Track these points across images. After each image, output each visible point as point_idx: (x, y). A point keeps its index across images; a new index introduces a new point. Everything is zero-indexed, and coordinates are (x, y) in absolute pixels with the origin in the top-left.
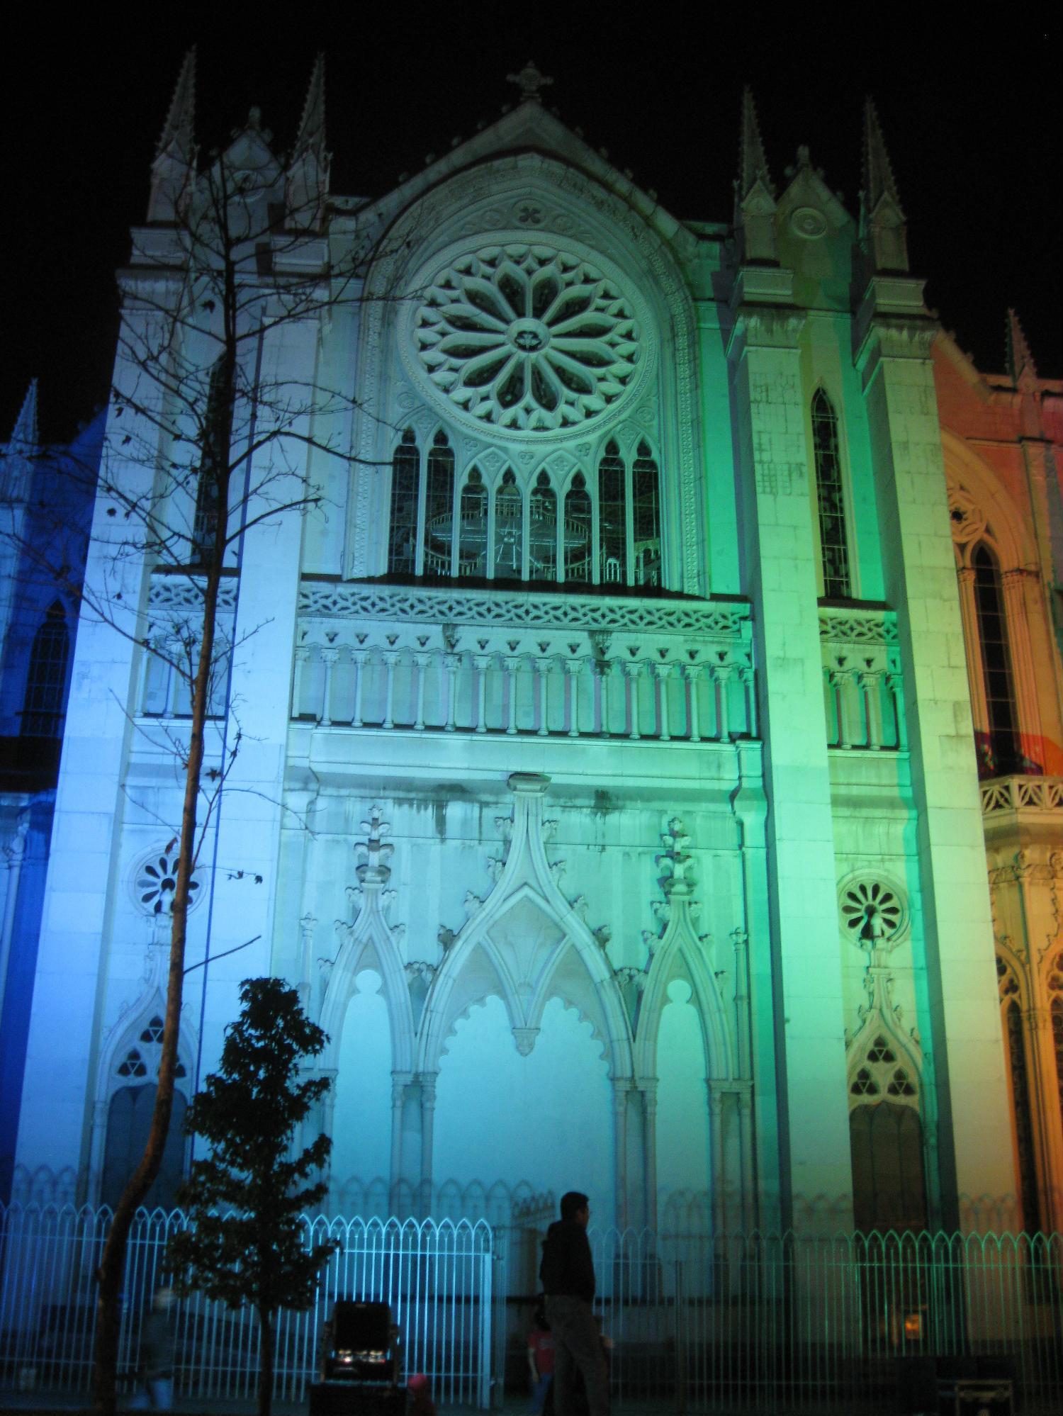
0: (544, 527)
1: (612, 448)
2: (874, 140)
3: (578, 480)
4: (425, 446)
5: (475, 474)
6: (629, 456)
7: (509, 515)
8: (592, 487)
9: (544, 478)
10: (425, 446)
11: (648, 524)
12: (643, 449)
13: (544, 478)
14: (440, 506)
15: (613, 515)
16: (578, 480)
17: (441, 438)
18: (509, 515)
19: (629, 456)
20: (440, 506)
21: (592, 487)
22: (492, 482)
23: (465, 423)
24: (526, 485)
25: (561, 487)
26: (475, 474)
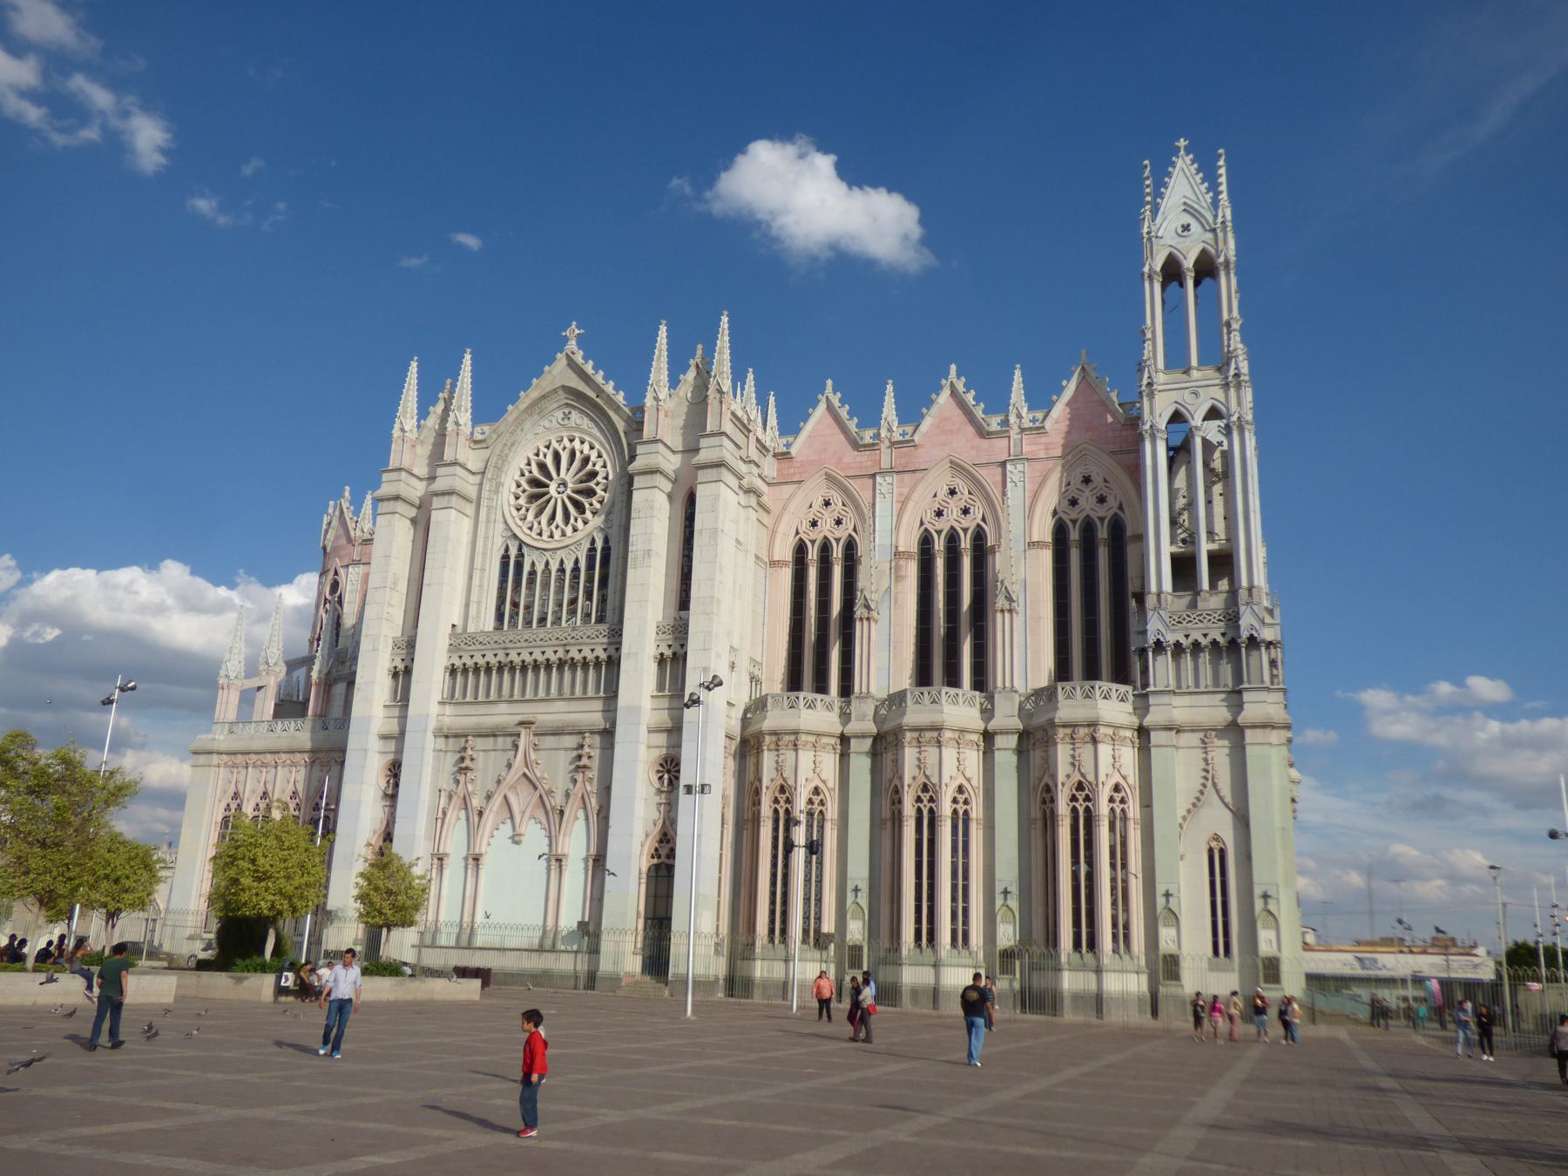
1: (593, 541)
2: (723, 342)
3: (577, 561)
4: (513, 553)
5: (533, 564)
7: (546, 585)
8: (583, 565)
9: (562, 562)
10: (513, 553)
12: (606, 540)
13: (562, 562)
16: (577, 561)
17: (520, 549)
18: (546, 585)
19: (599, 545)
22: (540, 568)
24: (554, 567)
25: (569, 566)
26: (533, 564)
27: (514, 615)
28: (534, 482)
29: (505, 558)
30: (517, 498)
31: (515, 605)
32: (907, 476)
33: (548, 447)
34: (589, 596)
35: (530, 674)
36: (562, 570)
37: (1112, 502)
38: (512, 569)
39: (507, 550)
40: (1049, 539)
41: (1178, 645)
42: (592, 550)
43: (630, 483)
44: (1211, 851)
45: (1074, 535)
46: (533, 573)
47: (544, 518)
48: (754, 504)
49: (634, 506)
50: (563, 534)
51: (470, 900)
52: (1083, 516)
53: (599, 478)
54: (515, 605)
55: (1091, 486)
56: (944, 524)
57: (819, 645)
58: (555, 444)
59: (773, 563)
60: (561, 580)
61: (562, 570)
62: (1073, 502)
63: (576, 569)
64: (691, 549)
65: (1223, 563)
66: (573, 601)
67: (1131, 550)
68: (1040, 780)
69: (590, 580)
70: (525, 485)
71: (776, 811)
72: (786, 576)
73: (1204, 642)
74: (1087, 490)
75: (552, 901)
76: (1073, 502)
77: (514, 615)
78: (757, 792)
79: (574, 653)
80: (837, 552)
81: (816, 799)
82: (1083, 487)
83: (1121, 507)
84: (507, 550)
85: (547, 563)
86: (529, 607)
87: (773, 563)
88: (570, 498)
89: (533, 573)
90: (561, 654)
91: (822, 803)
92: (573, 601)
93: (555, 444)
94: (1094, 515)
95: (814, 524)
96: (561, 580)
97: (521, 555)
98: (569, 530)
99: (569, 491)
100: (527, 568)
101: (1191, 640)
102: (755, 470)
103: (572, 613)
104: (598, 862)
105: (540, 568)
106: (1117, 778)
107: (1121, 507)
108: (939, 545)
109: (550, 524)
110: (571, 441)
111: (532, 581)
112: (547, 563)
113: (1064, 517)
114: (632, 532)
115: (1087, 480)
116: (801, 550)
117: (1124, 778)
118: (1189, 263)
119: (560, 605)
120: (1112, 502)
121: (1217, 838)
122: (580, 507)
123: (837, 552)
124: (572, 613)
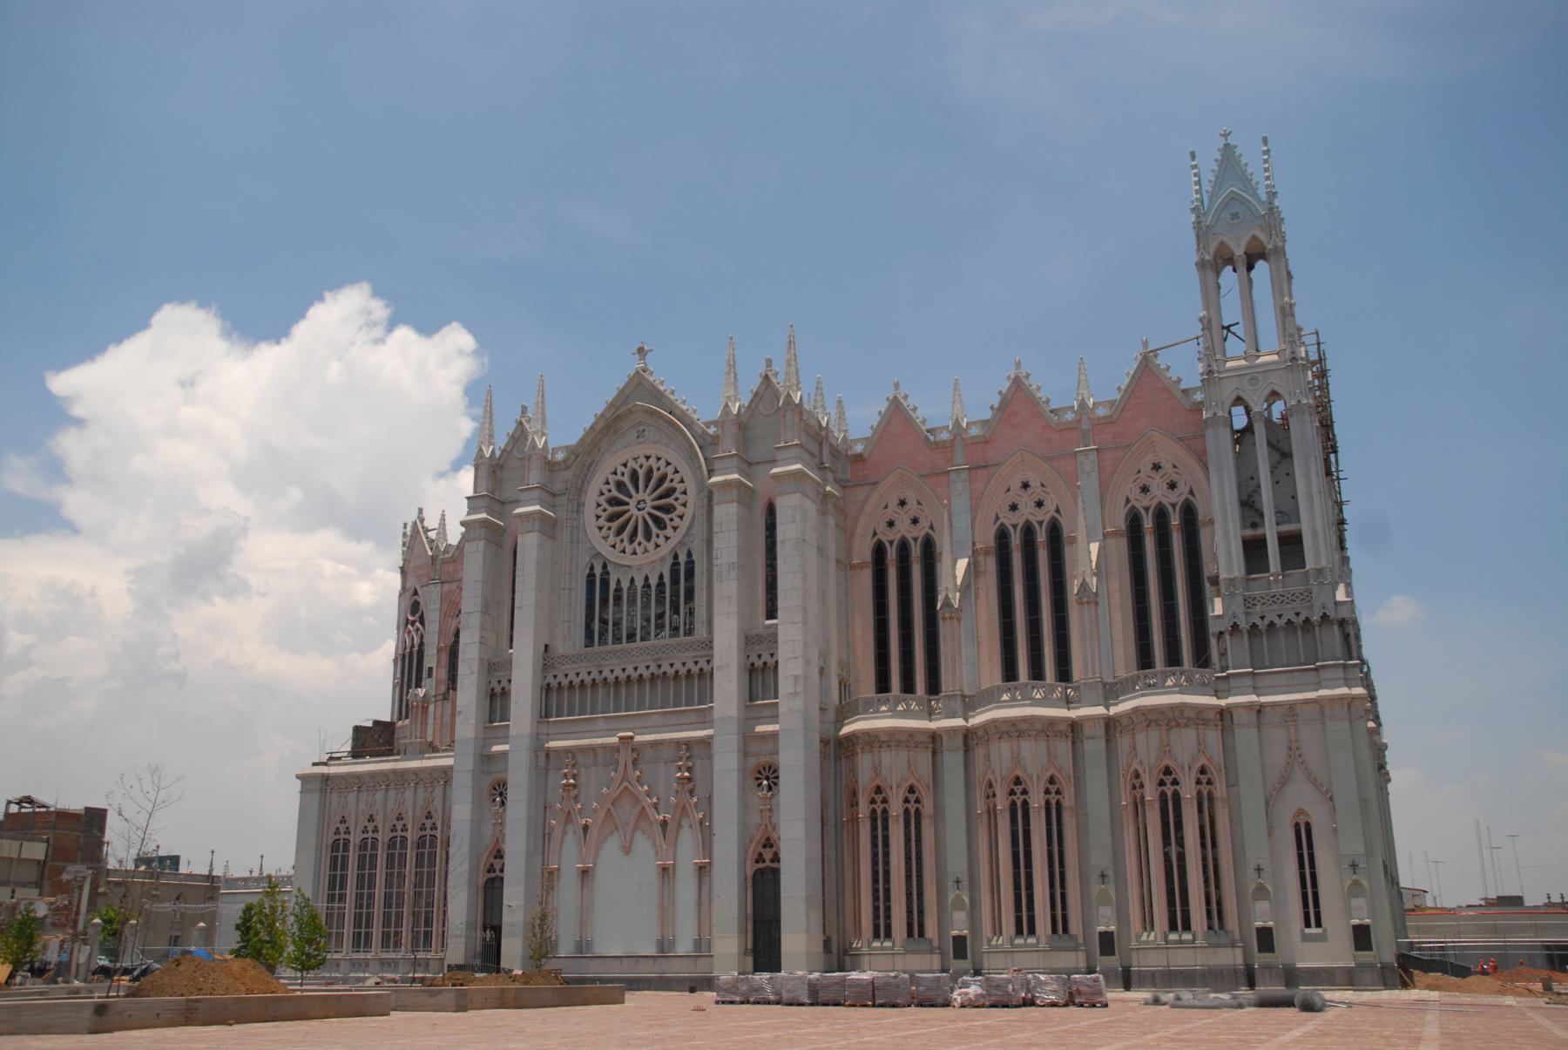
0: (646, 606)
1: (676, 557)
3: (661, 577)
4: (598, 571)
6: (682, 559)
7: (632, 601)
8: (667, 580)
9: (647, 578)
10: (598, 571)
11: (690, 594)
12: (689, 554)
13: (647, 578)
14: (604, 601)
15: (675, 594)
16: (661, 577)
17: (605, 566)
18: (632, 601)
19: (682, 559)
20: (604, 601)
21: (667, 580)
22: (625, 585)
23: (613, 556)
24: (639, 583)
25: (653, 582)
27: (603, 633)
28: (614, 502)
29: (591, 576)
30: (598, 517)
31: (604, 622)
32: (980, 473)
33: (625, 465)
34: (675, 609)
35: (624, 689)
36: (647, 585)
37: (1183, 489)
38: (599, 588)
39: (592, 568)
40: (1123, 527)
41: (1254, 626)
42: (675, 564)
43: (710, 499)
44: (1297, 825)
45: (1148, 523)
46: (618, 590)
47: (625, 535)
48: (830, 507)
49: (716, 520)
50: (646, 551)
51: (584, 915)
52: (1155, 502)
53: (677, 494)
54: (604, 622)
55: (1161, 472)
56: (1018, 519)
57: (903, 646)
58: (631, 464)
59: (853, 567)
60: (646, 595)
61: (647, 585)
62: (1145, 489)
63: (661, 584)
64: (775, 559)
65: (1292, 544)
66: (660, 616)
67: (1204, 534)
68: (1129, 765)
69: (675, 594)
70: (605, 505)
71: (874, 811)
72: (866, 578)
73: (1279, 623)
74: (1157, 476)
75: (666, 911)
76: (1145, 489)
77: (603, 633)
78: (854, 794)
79: (665, 667)
80: (916, 551)
81: (912, 797)
82: (1153, 473)
83: (1191, 492)
84: (592, 568)
85: (632, 580)
86: (617, 624)
87: (853, 567)
88: (650, 514)
89: (618, 590)
90: (653, 669)
91: (917, 801)
92: (660, 616)
93: (631, 464)
94: (1166, 502)
95: (891, 524)
96: (646, 595)
97: (605, 573)
98: (651, 546)
99: (648, 509)
100: (612, 586)
101: (1267, 621)
102: (830, 476)
103: (660, 627)
104: (703, 870)
105: (625, 585)
106: (1203, 761)
107: (1191, 492)
108: (1016, 540)
109: (631, 541)
110: (648, 458)
111: (618, 598)
112: (632, 580)
113: (1138, 505)
114: (716, 545)
115: (1157, 467)
116: (879, 551)
117: (1209, 760)
118: (1239, 252)
119: (648, 620)
120: (1183, 489)
121: (1301, 812)
122: (660, 524)
123: (916, 551)
124: (660, 627)
